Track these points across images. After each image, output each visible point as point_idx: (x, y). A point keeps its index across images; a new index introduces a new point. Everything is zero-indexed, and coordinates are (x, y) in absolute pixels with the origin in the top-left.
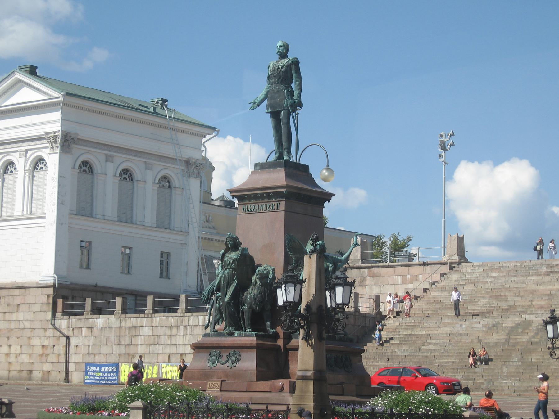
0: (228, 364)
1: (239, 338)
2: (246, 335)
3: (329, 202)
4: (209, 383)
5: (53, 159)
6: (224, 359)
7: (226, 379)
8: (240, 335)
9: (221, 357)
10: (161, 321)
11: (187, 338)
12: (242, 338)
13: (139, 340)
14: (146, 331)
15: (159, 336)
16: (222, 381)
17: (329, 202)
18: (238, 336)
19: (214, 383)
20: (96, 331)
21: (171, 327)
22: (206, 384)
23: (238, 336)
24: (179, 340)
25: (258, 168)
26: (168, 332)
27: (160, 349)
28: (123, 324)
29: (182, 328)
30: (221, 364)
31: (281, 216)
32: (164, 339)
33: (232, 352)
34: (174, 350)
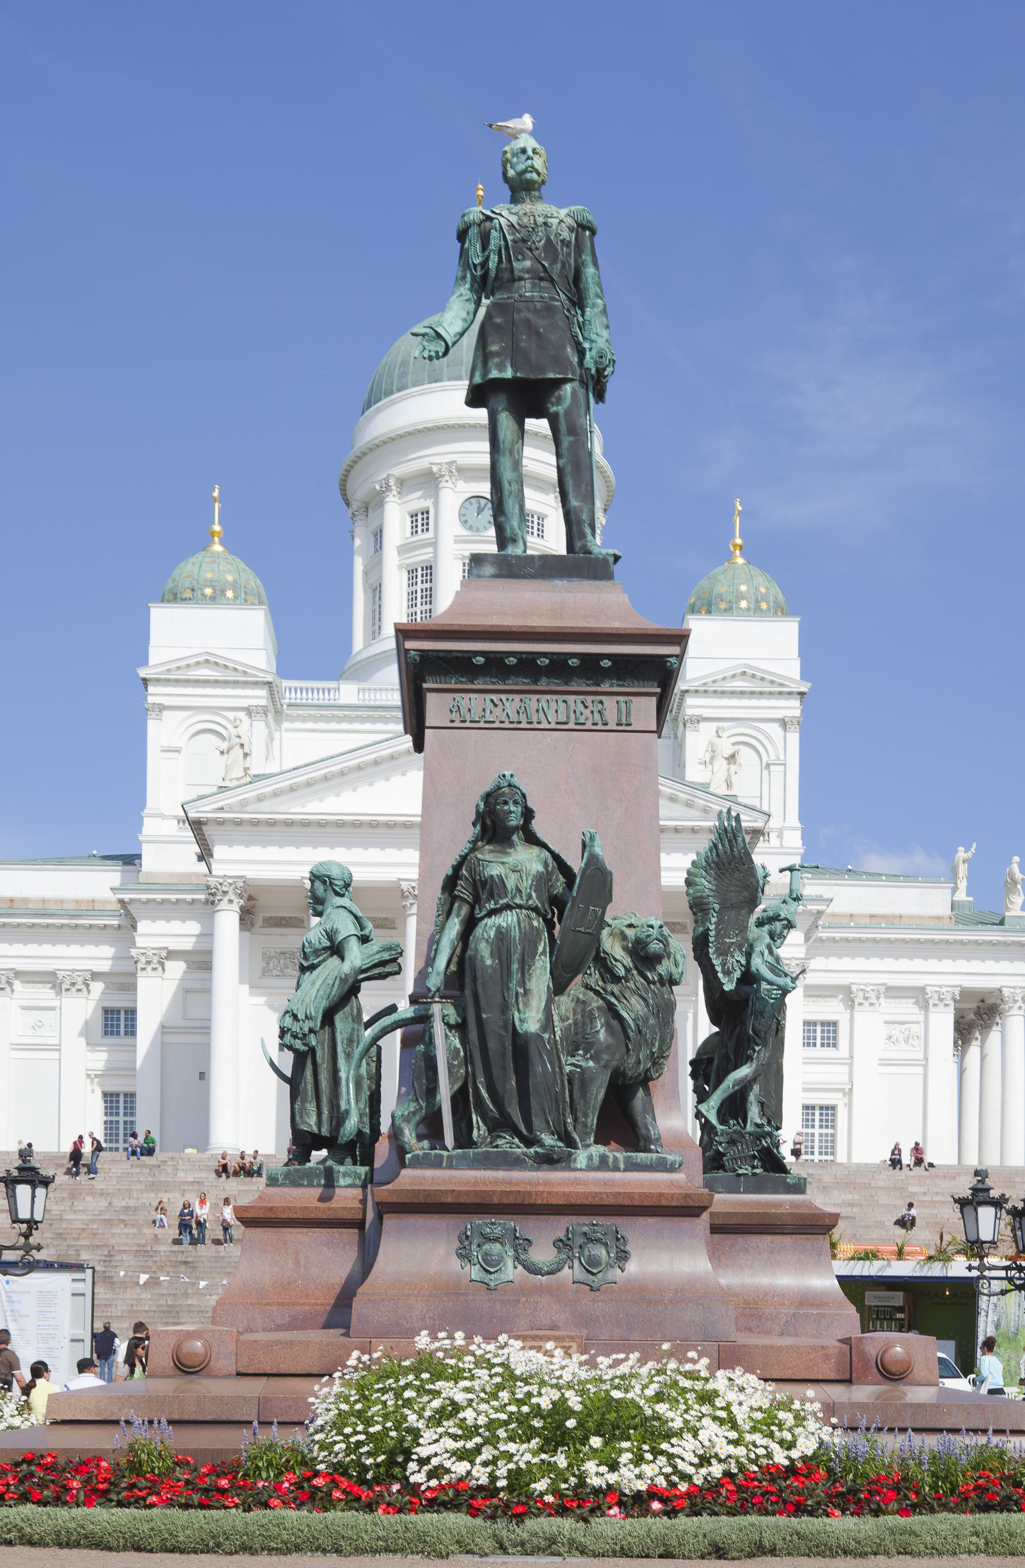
1: (600, 1175)
6: (543, 1254)
8: (603, 1164)
9: (521, 1245)
12: (617, 1175)
23: (590, 1168)
30: (532, 1269)
33: (583, 1223)
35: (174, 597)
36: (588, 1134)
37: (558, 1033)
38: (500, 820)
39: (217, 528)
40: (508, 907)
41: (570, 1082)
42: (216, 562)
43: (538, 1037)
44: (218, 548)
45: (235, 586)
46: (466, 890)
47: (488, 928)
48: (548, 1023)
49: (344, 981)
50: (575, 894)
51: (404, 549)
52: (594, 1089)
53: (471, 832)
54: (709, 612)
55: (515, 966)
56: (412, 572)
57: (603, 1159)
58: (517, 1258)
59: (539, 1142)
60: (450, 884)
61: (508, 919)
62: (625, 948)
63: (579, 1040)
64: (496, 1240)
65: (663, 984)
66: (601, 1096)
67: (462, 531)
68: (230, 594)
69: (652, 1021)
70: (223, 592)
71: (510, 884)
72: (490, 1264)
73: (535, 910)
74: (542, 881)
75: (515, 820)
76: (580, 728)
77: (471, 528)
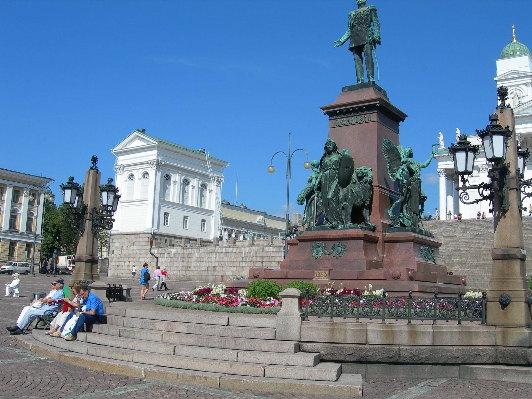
0: (333, 255)
2: (350, 228)
3: (403, 121)
4: (316, 272)
5: (152, 172)
7: (333, 268)
8: (344, 228)
10: (204, 251)
11: (217, 258)
13: (193, 260)
14: (197, 255)
15: (203, 258)
16: (330, 270)
17: (403, 121)
18: (341, 229)
19: (321, 271)
20: (172, 255)
21: (209, 253)
22: (313, 273)
24: (213, 260)
25: (346, 90)
26: (207, 255)
27: (203, 264)
28: (185, 252)
29: (214, 254)
31: (374, 126)
32: (205, 259)
33: (337, 243)
34: (210, 265)
35: (503, 57)
36: (349, 221)
37: (341, 197)
39: (514, 36)
40: (328, 169)
41: (343, 209)
42: (515, 45)
44: (515, 41)
49: (311, 187)
50: (347, 163)
52: (348, 210)
55: (328, 183)
57: (344, 226)
58: (323, 251)
63: (345, 199)
64: (319, 247)
65: (365, 183)
66: (351, 211)
69: (361, 192)
70: (516, 53)
71: (328, 164)
72: (318, 253)
73: (334, 169)
76: (360, 123)
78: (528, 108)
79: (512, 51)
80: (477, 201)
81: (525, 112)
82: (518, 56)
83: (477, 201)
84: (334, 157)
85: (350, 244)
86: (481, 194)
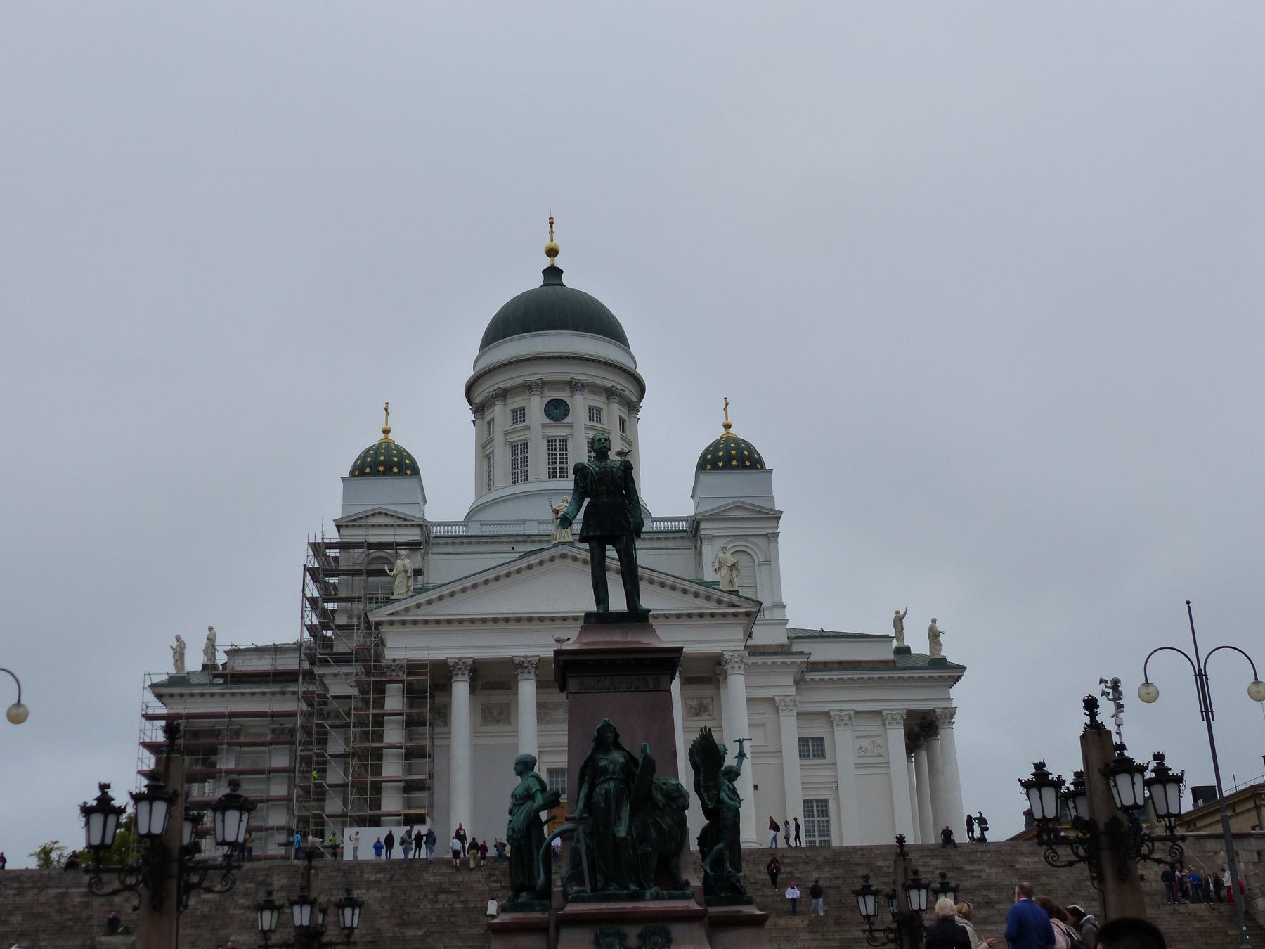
8: (657, 897)
9: (623, 937)
38: (605, 740)
43: (624, 839)
45: (399, 464)
46: (589, 772)
47: (601, 789)
48: (629, 832)
51: (506, 434)
53: (592, 745)
54: (712, 468)
55: (613, 807)
56: (514, 448)
57: (657, 894)
59: (627, 888)
60: (584, 769)
61: (611, 785)
62: (663, 795)
67: (548, 421)
68: (395, 470)
70: (391, 469)
74: (625, 767)
75: (611, 740)
77: (552, 419)
78: (429, 602)
79: (382, 463)
80: (1071, 864)
81: (419, 611)
82: (395, 474)
83: (1071, 864)
84: (618, 757)
85: (676, 930)
86: (1076, 854)
